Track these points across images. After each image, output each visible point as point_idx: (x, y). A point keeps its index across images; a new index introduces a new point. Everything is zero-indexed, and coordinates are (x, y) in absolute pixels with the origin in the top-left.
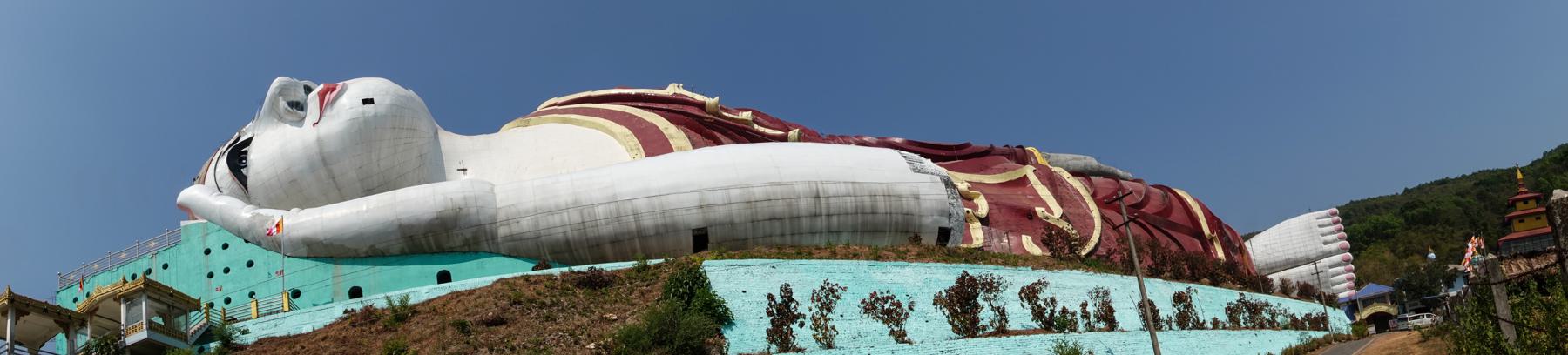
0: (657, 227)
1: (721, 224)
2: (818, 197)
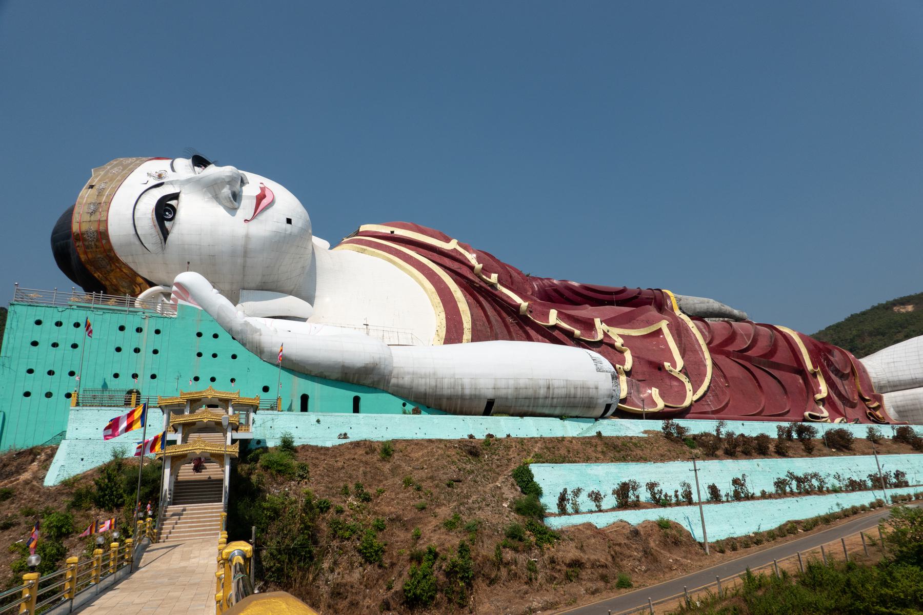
0: (471, 395)
1: (501, 398)
2: (549, 388)
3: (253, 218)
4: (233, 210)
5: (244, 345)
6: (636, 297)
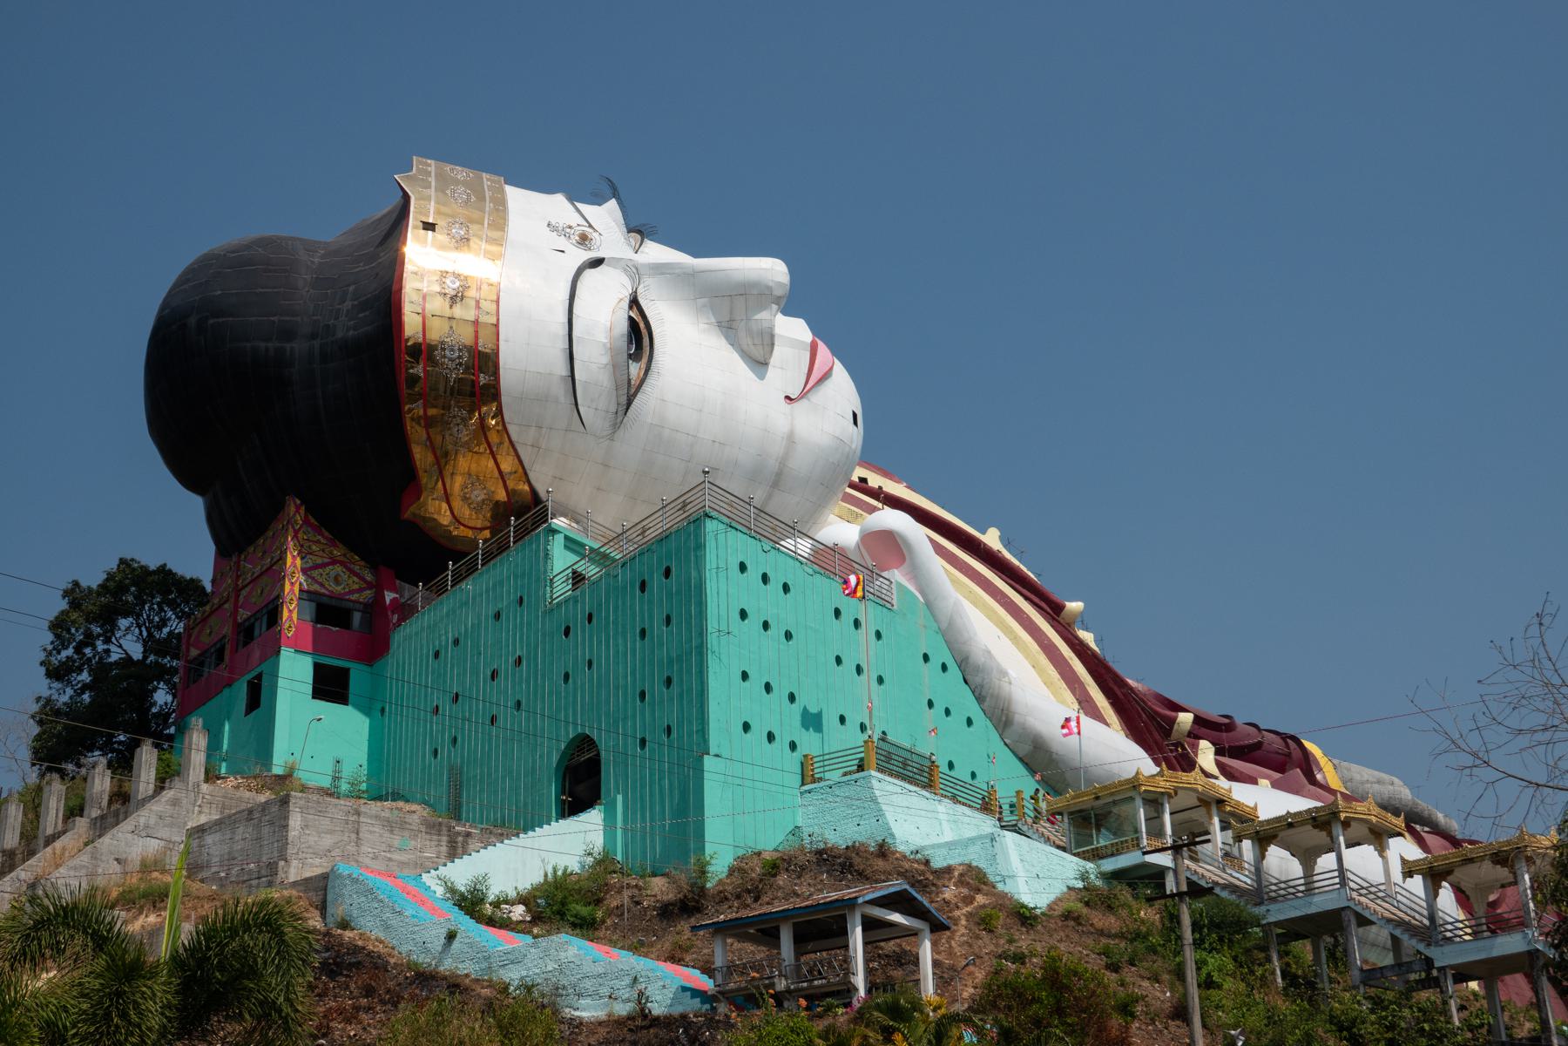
3: (803, 395)
4: (759, 364)
5: (980, 699)
6: (1259, 745)
